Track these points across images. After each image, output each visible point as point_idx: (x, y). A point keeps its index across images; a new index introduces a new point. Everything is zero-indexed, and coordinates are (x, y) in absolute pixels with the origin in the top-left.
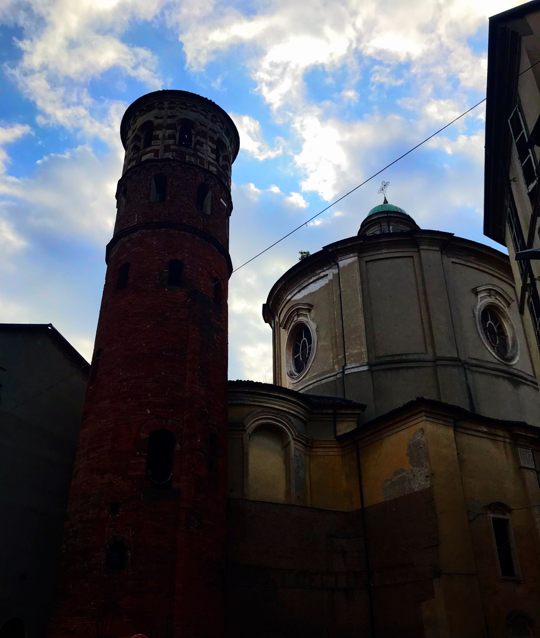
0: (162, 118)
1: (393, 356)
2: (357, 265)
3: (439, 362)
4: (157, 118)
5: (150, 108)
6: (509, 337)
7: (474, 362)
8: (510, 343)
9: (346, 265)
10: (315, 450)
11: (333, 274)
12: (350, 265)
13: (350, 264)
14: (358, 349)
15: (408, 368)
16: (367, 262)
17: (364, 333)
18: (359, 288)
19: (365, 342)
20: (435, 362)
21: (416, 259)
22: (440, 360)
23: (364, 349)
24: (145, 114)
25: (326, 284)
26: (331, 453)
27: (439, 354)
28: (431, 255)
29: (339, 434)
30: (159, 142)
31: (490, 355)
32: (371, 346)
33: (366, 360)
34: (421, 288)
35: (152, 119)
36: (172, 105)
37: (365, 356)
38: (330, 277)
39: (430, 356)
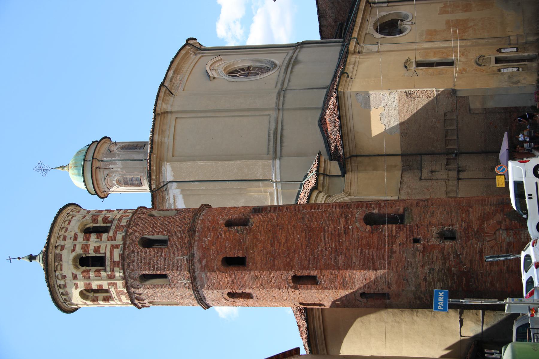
0: (75, 246)
1: (269, 141)
2: (176, 164)
3: (281, 106)
4: (73, 250)
5: (59, 258)
6: (252, 64)
7: (279, 85)
8: (257, 64)
9: (173, 174)
10: (352, 191)
11: (176, 188)
12: (173, 169)
13: (172, 170)
14: (258, 168)
15: (282, 129)
16: (173, 156)
17: (244, 162)
18: (199, 163)
19: (254, 162)
20: (279, 110)
21: (179, 115)
22: (278, 105)
23: (260, 162)
24: (61, 265)
25: (183, 198)
26: (356, 180)
27: (273, 106)
28: (173, 104)
29: (340, 173)
30: (103, 246)
31: (272, 75)
32: (257, 157)
33: (270, 161)
34: (209, 114)
35: (74, 254)
36: (62, 237)
37: (266, 162)
38: (178, 191)
39: (273, 114)
